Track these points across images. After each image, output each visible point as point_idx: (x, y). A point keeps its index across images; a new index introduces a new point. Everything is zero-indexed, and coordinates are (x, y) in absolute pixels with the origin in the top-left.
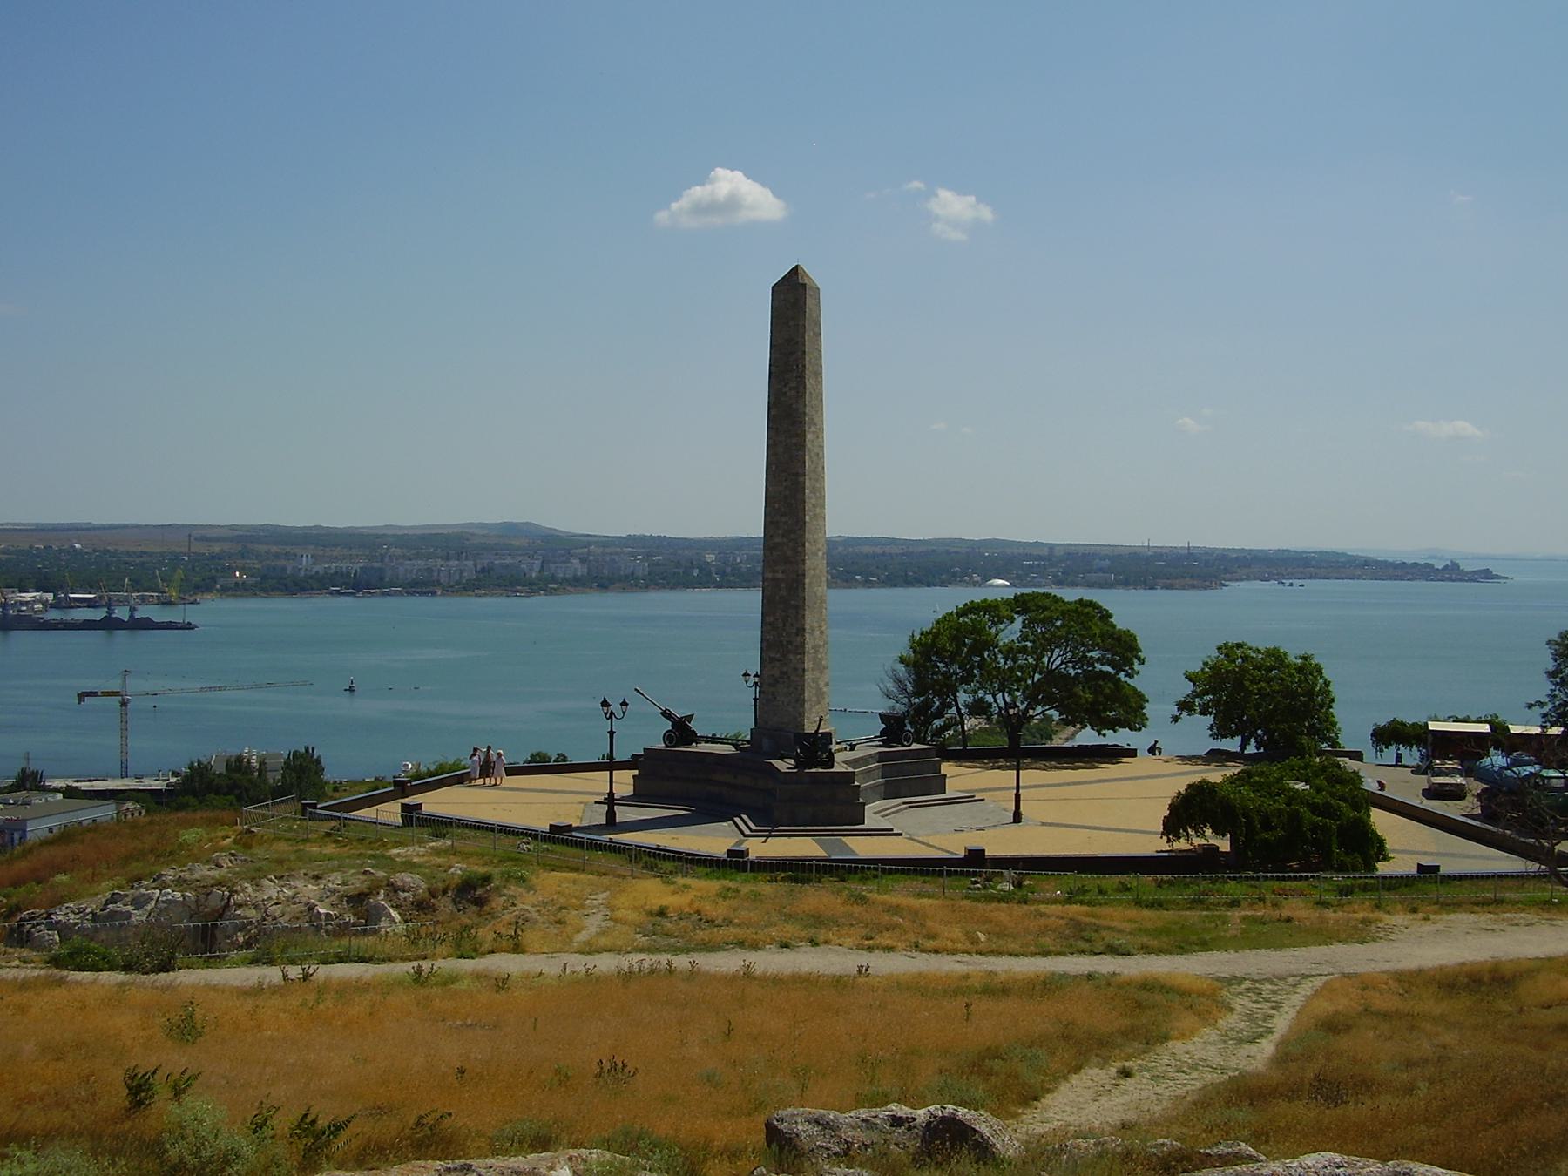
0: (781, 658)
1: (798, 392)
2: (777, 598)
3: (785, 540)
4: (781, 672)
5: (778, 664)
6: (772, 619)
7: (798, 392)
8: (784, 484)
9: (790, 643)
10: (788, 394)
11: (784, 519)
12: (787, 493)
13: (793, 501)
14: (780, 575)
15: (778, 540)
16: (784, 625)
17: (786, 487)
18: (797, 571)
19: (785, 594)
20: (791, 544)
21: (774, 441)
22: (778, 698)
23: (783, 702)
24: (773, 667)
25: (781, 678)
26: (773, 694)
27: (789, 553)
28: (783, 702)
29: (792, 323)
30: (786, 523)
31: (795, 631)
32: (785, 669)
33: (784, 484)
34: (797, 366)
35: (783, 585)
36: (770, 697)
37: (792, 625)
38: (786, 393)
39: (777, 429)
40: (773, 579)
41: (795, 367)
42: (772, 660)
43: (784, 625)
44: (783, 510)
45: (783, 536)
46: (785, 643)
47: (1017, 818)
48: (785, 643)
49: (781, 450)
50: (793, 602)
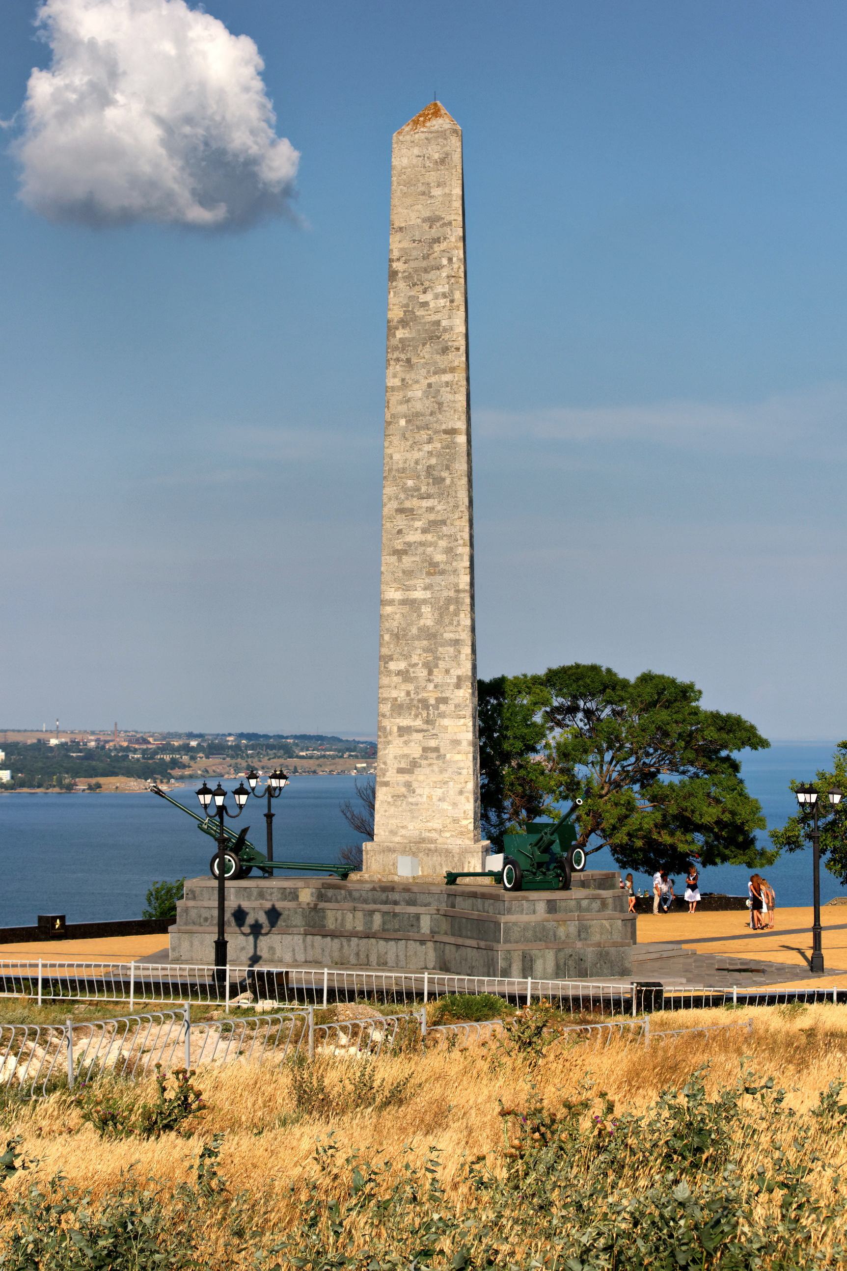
0: (425, 727)
1: (452, 301)
2: (414, 630)
3: (429, 537)
4: (425, 750)
5: (419, 736)
6: (402, 665)
7: (452, 301)
8: (428, 448)
9: (445, 700)
10: (432, 305)
11: (426, 503)
12: (433, 461)
13: (445, 474)
14: (419, 594)
15: (414, 537)
16: (430, 673)
17: (430, 453)
18: (457, 585)
19: (429, 623)
20: (443, 543)
21: (403, 380)
22: (418, 791)
23: (430, 797)
24: (406, 743)
25: (426, 758)
26: (408, 785)
27: (439, 557)
28: (430, 797)
29: (437, 192)
30: (431, 509)
31: (455, 680)
32: (432, 743)
33: (428, 448)
34: (450, 260)
35: (426, 609)
36: (403, 790)
37: (447, 671)
38: (425, 304)
39: (408, 361)
40: (404, 602)
41: (445, 261)
42: (403, 731)
43: (430, 673)
44: (424, 489)
45: (424, 531)
46: (432, 701)
47: (816, 965)
48: (432, 701)
49: (419, 394)
50: (448, 636)
